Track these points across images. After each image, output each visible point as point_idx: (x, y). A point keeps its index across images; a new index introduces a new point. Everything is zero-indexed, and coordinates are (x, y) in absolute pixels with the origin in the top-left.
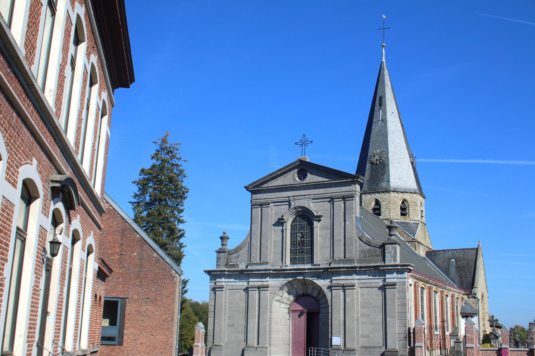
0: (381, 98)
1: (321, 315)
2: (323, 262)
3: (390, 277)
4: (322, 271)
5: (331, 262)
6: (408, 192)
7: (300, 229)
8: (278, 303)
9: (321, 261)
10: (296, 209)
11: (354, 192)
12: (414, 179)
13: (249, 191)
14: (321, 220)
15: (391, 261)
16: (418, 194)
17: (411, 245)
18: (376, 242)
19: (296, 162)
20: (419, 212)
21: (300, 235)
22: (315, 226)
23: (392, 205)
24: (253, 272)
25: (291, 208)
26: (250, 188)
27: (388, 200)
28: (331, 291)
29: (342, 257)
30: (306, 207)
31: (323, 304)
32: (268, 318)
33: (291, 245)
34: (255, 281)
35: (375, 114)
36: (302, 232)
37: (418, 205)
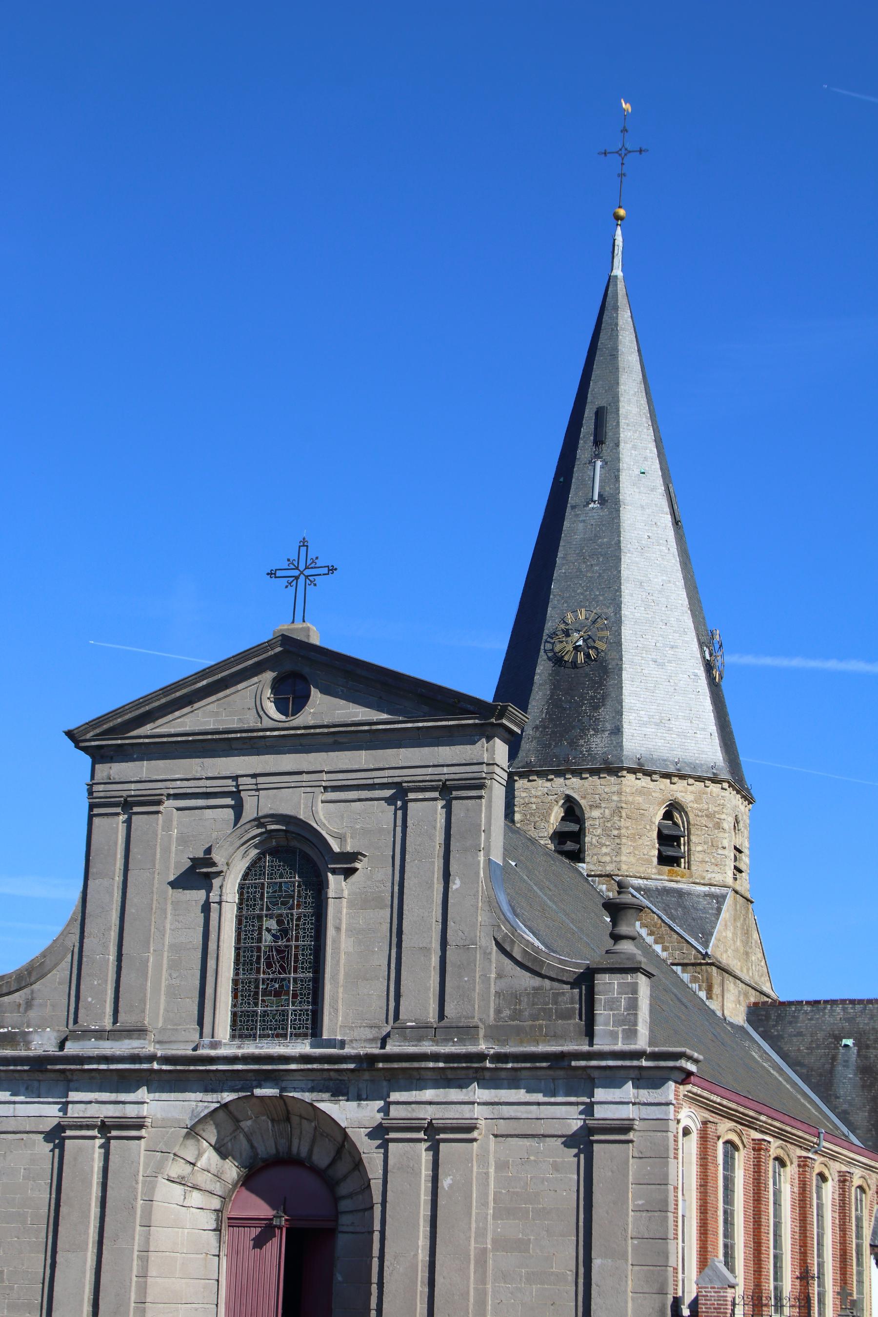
0: (600, 414)
1: (342, 1241)
2: (356, 1034)
3: (610, 1099)
4: (352, 1066)
5: (388, 1035)
6: (690, 776)
7: (275, 904)
8: (179, 1189)
9: (351, 1028)
10: (261, 825)
11: (485, 768)
12: (714, 728)
13: (85, 750)
14: (356, 870)
15: (614, 1035)
16: (726, 785)
17: (694, 980)
18: (561, 962)
19: (270, 644)
20: (726, 852)
21: (272, 924)
22: (331, 893)
24: (86, 1067)
25: (242, 821)
26: (88, 736)
27: (613, 805)
28: (384, 1146)
29: (432, 1016)
30: (301, 817)
31: (350, 1196)
32: (136, 1248)
33: (237, 962)
34: (90, 1102)
35: (575, 475)
36: (281, 915)
37: (726, 825)
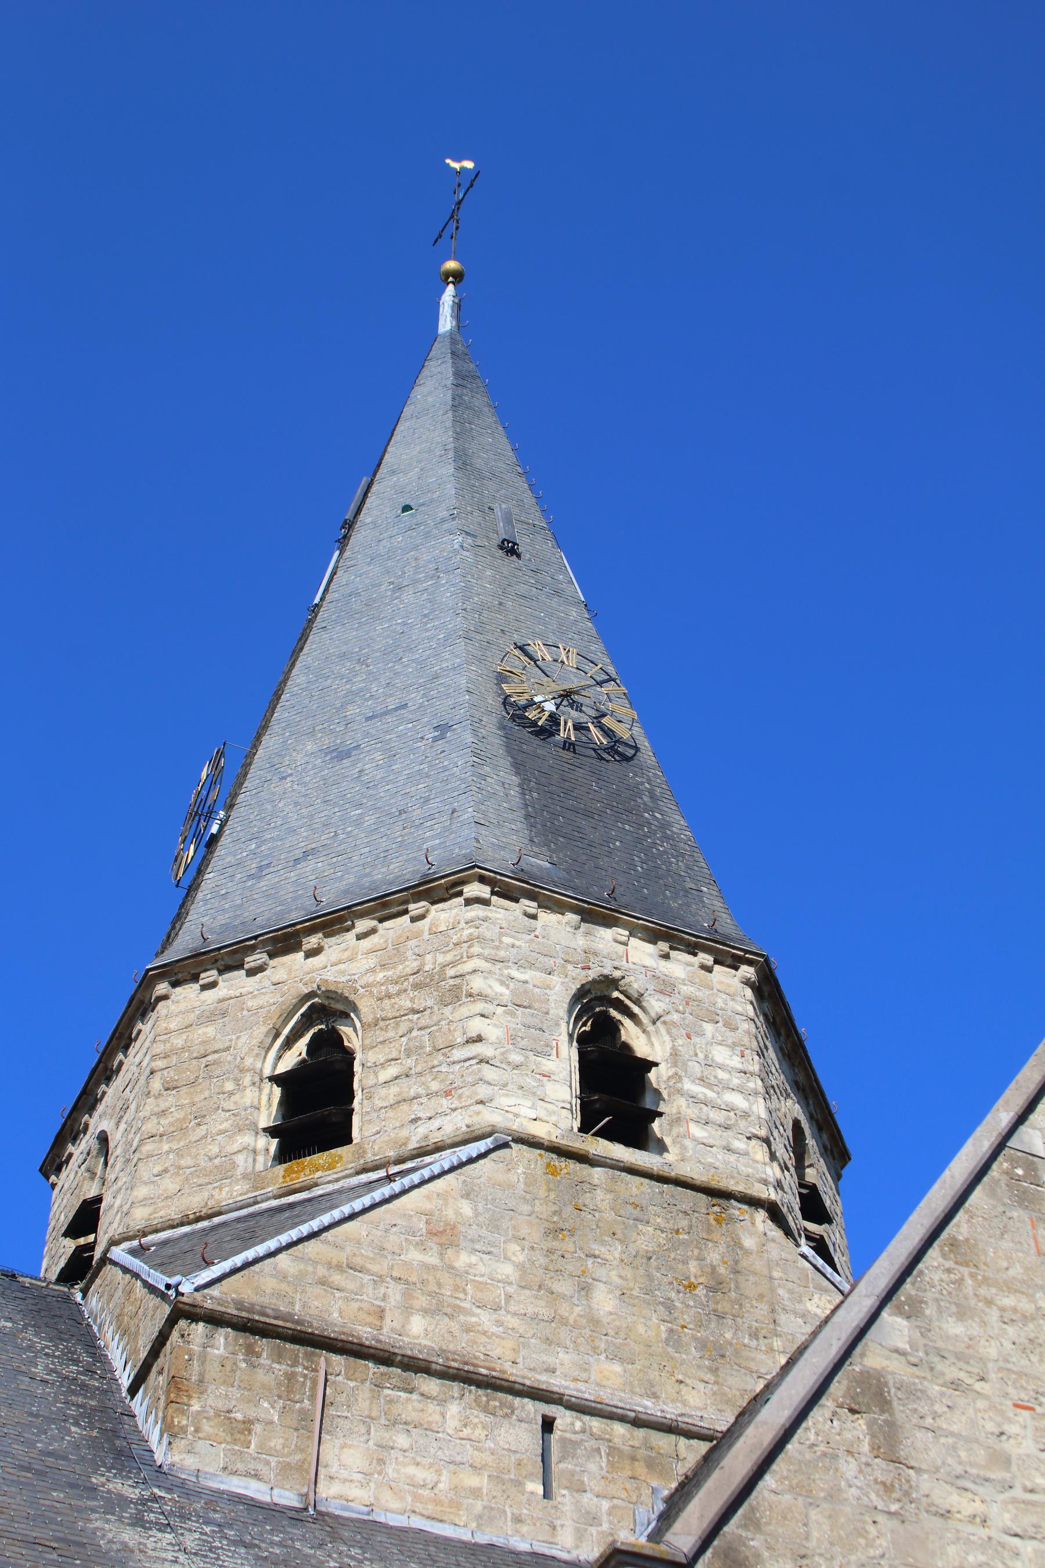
23: (170, 1100)
